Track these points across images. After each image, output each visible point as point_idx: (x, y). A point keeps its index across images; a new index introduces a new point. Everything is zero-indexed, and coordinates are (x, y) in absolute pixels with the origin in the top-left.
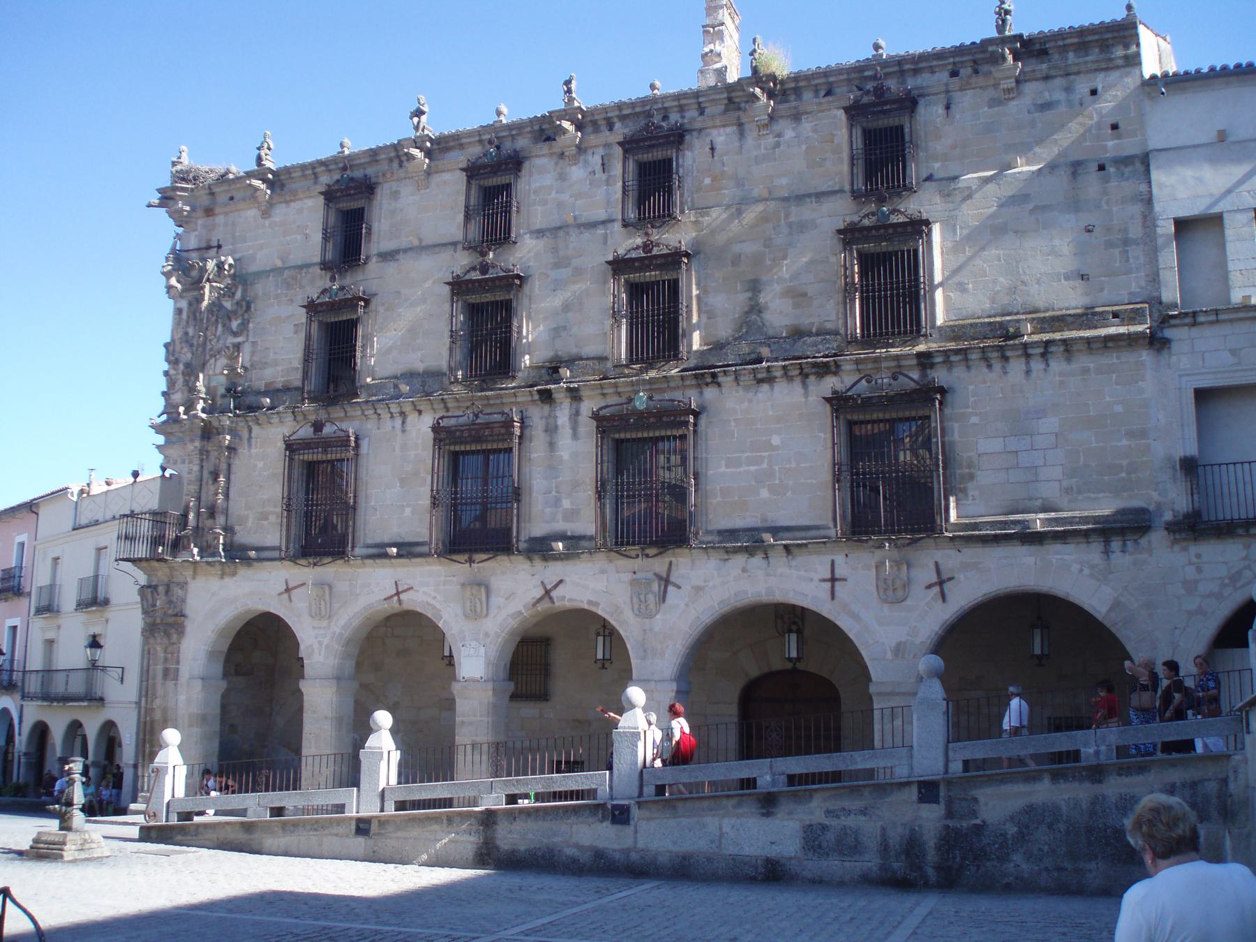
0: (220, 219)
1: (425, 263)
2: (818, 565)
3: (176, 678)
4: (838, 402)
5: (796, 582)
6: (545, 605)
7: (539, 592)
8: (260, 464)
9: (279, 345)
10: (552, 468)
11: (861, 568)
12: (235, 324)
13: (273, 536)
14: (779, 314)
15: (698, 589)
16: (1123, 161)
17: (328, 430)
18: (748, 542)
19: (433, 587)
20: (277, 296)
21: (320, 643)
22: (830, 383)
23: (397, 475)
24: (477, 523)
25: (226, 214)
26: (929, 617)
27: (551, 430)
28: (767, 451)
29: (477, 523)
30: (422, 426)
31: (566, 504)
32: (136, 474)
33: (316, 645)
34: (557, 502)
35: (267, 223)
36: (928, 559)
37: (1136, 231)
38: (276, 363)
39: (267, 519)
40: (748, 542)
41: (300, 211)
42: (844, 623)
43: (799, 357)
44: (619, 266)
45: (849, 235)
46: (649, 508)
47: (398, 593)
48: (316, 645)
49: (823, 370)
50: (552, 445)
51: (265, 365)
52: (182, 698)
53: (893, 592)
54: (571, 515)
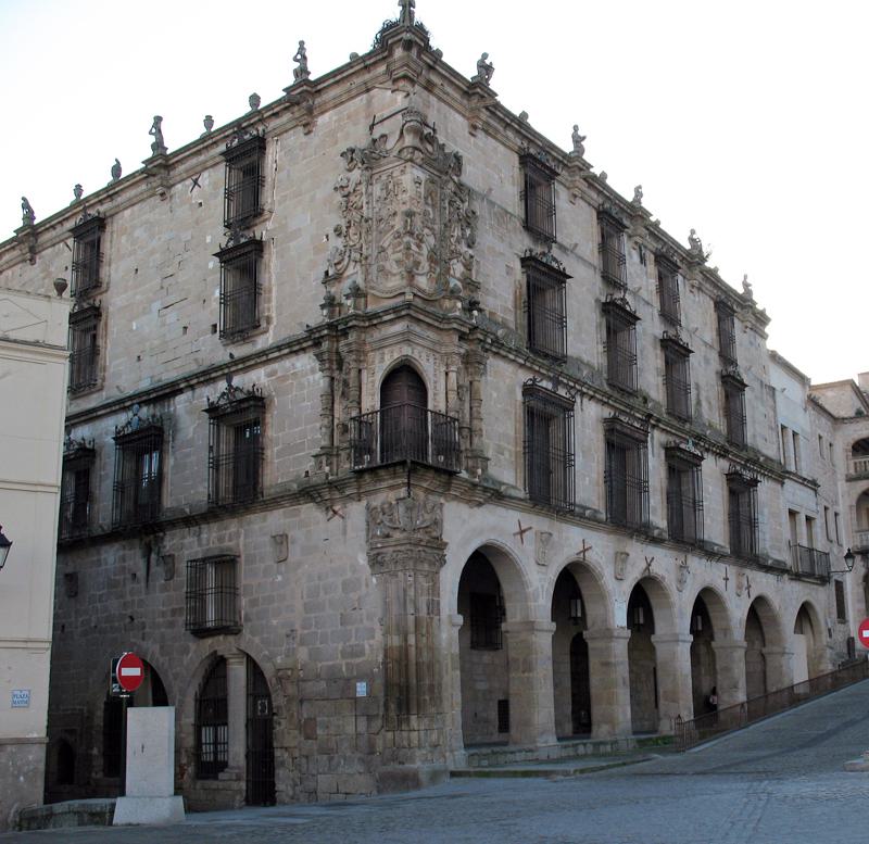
3: (439, 614)
6: (647, 574)
7: (644, 565)
8: (495, 395)
20: (491, 226)
21: (542, 587)
25: (440, 99)
33: (540, 590)
35: (472, 139)
39: (503, 454)
47: (584, 551)
48: (540, 590)
52: (444, 636)
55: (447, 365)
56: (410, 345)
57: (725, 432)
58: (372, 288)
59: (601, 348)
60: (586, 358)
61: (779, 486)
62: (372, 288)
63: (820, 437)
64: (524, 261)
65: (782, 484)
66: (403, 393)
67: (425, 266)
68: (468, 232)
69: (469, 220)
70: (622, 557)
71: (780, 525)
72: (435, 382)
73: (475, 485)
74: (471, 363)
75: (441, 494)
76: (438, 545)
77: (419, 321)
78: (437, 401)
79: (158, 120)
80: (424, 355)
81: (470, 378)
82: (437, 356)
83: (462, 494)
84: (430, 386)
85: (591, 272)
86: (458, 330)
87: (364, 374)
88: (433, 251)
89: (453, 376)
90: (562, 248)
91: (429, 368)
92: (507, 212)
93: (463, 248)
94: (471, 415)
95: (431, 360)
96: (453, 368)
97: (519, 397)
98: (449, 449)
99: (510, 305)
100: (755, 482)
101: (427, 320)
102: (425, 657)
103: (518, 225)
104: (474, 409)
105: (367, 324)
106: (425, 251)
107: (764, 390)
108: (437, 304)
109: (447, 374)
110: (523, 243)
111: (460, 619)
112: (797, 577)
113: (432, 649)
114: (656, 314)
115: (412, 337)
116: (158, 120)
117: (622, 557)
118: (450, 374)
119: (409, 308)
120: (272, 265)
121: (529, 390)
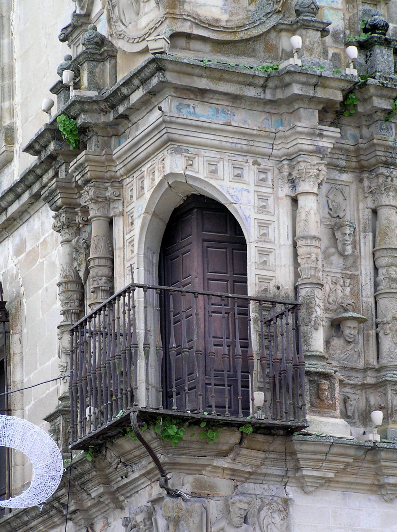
55: (293, 182)
56: (178, 151)
58: (120, 36)
62: (120, 36)
66: (194, 264)
72: (263, 225)
73: (373, 449)
75: (284, 480)
77: (201, 94)
78: (269, 268)
80: (225, 169)
81: (370, 203)
82: (265, 163)
83: (338, 472)
84: (251, 233)
86: (311, 99)
87: (119, 225)
89: (309, 205)
94: (376, 285)
95: (250, 174)
96: (305, 186)
98: (294, 381)
101: (223, 87)
104: (382, 271)
105: (111, 117)
108: (260, 47)
109: (295, 200)
115: (177, 133)
118: (302, 201)
119: (160, 69)
120: (14, 16)
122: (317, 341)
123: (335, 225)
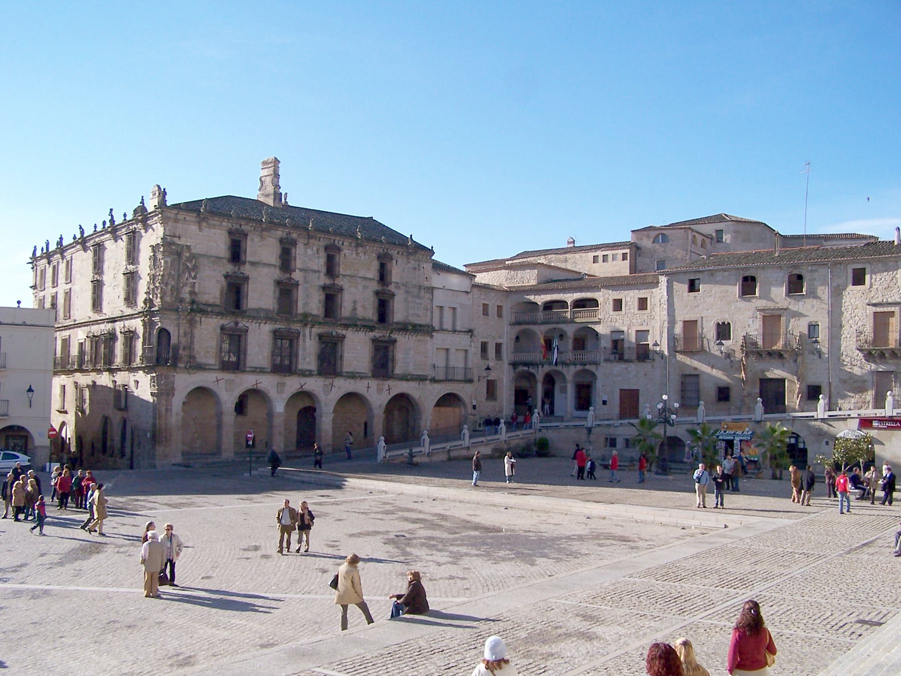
0: (179, 225)
1: (266, 270)
2: (365, 382)
4: (374, 341)
5: (358, 386)
9: (211, 287)
10: (304, 349)
11: (374, 383)
12: (193, 274)
13: (212, 361)
14: (360, 313)
15: (339, 388)
16: (429, 288)
17: (240, 325)
18: (353, 376)
19: (267, 383)
22: (372, 334)
23: (259, 342)
24: (284, 365)
26: (385, 398)
27: (304, 336)
28: (357, 350)
29: (284, 365)
30: (267, 328)
31: (308, 359)
32: (19, 302)
34: (305, 359)
36: (391, 383)
37: (429, 306)
38: (209, 294)
40: (353, 376)
41: (215, 234)
42: (369, 398)
43: (368, 327)
44: (324, 288)
45: (377, 293)
46: (329, 362)
49: (372, 331)
50: (304, 340)
51: (205, 294)
53: (380, 391)
54: (309, 363)
57: (376, 318)
59: (275, 301)
60: (264, 307)
61: (429, 338)
63: (485, 306)
64: (226, 276)
65: (432, 336)
67: (169, 293)
68: (193, 274)
69: (195, 268)
70: (281, 386)
71: (426, 357)
74: (192, 323)
76: (173, 389)
78: (174, 340)
79: (111, 210)
85: (272, 269)
88: (172, 287)
90: (253, 264)
91: (171, 329)
92: (218, 258)
93: (191, 280)
97: (219, 331)
99: (218, 296)
100: (395, 341)
102: (163, 426)
103: (225, 261)
106: (169, 287)
107: (422, 291)
110: (230, 268)
111: (182, 414)
112: (434, 380)
113: (166, 424)
114: (322, 275)
116: (111, 210)
117: (281, 386)
121: (223, 328)
122: (181, 352)
123: (185, 333)
